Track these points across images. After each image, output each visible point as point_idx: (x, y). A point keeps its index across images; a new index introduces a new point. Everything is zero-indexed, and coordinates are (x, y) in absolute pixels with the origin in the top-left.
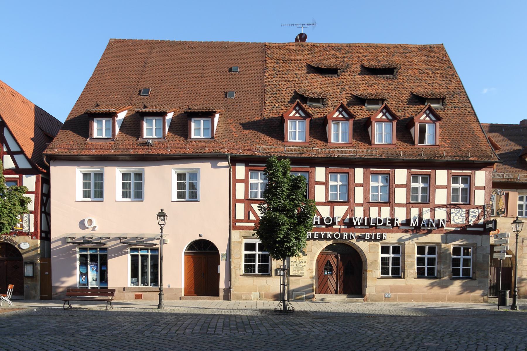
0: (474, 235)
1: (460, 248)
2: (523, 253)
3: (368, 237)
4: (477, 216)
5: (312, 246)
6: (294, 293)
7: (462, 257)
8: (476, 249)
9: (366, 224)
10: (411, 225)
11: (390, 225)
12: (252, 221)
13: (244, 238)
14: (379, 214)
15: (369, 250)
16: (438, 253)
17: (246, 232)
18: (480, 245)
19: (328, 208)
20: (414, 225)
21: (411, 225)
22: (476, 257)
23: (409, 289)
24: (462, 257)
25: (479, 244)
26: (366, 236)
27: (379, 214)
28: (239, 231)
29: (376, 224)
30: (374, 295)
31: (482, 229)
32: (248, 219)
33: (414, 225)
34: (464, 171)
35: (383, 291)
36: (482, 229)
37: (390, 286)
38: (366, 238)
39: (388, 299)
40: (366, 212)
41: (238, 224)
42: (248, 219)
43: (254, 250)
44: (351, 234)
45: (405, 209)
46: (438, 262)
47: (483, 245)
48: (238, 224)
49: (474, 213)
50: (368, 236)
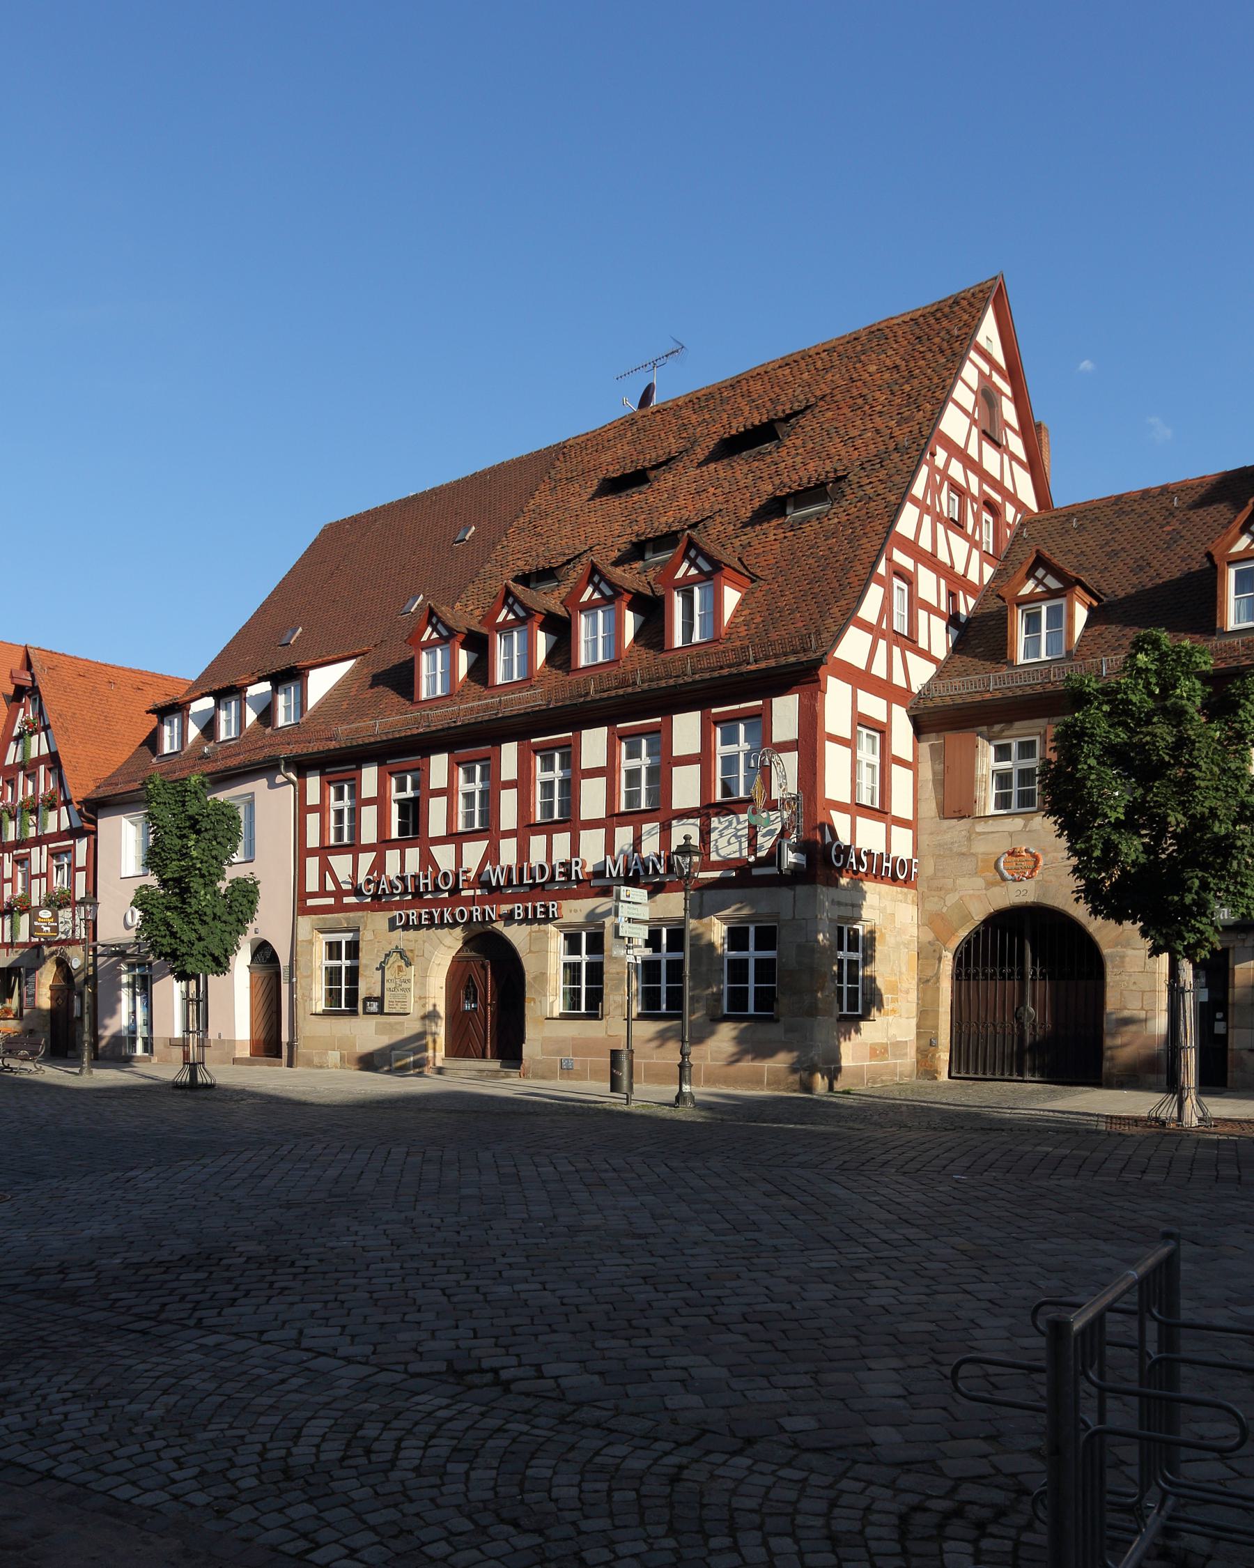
0: (774, 889)
1: (748, 928)
2: (1124, 930)
3: (519, 915)
4: (778, 832)
5: (424, 942)
6: (394, 1053)
7: (752, 954)
10: (608, 876)
11: (563, 879)
12: (329, 894)
13: (322, 932)
14: (575, 850)
18: (789, 917)
19: (451, 848)
21: (608, 876)
24: (752, 954)
25: (786, 915)
26: (516, 911)
27: (575, 850)
30: (540, 1062)
32: (323, 893)
33: (614, 874)
34: (742, 706)
35: (559, 1053)
37: (573, 1039)
38: (516, 918)
39: (568, 1074)
40: (523, 853)
41: (310, 902)
44: (487, 908)
48: (310, 902)
50: (520, 911)
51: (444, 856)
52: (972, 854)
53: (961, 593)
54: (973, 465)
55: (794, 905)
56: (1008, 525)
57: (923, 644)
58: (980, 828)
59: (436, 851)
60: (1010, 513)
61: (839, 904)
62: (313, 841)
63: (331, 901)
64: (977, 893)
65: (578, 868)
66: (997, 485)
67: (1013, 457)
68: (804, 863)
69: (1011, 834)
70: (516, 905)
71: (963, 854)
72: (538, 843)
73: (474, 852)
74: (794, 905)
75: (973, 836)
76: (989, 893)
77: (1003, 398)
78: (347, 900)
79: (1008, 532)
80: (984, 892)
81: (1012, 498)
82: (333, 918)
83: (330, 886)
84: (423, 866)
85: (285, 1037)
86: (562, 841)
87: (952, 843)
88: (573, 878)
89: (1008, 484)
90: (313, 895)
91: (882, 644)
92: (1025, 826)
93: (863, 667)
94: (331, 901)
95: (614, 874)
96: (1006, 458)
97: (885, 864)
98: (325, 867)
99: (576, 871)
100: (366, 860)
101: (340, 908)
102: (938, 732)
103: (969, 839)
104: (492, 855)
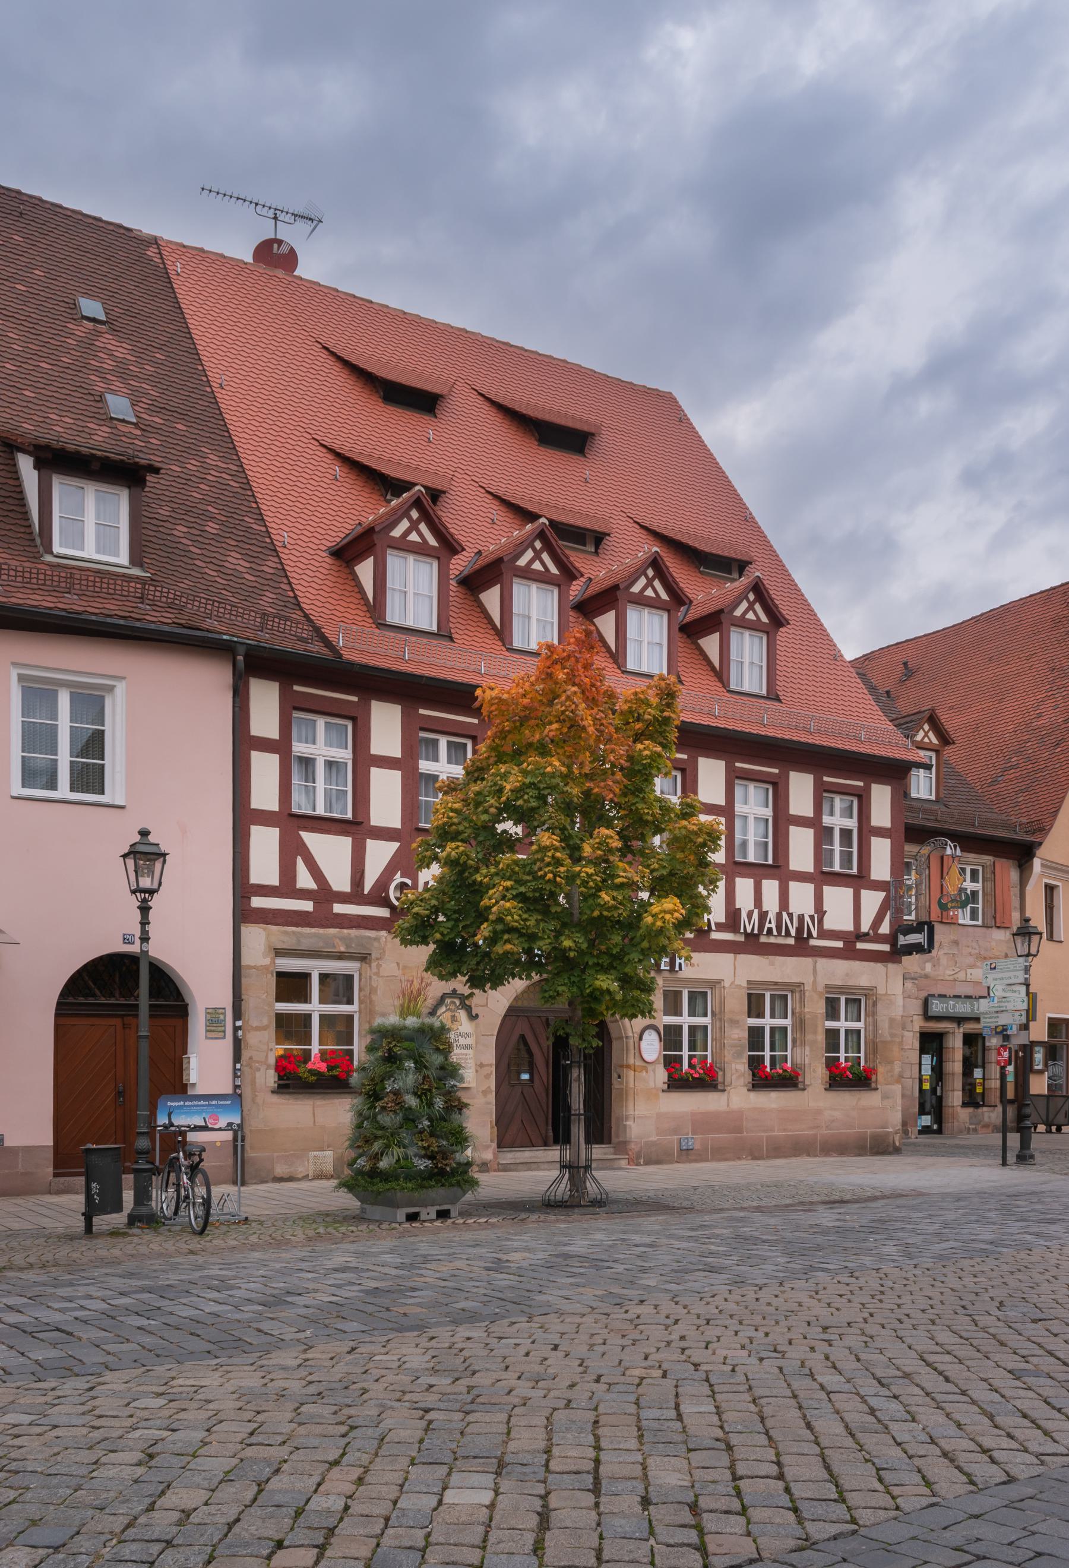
8: (875, 1004)
10: (742, 930)
12: (304, 894)
16: (793, 1013)
17: (286, 933)
20: (749, 930)
22: (875, 1024)
23: (733, 1123)
28: (264, 929)
30: (654, 1143)
31: (886, 948)
32: (287, 887)
33: (749, 930)
35: (675, 1131)
36: (886, 948)
37: (693, 1114)
39: (688, 1155)
41: (257, 902)
42: (287, 887)
43: (305, 998)
46: (794, 1041)
48: (257, 902)
63: (307, 906)
78: (339, 908)
82: (315, 935)
83: (305, 880)
88: (742, 930)
90: (343, 898)
94: (307, 906)
101: (322, 918)
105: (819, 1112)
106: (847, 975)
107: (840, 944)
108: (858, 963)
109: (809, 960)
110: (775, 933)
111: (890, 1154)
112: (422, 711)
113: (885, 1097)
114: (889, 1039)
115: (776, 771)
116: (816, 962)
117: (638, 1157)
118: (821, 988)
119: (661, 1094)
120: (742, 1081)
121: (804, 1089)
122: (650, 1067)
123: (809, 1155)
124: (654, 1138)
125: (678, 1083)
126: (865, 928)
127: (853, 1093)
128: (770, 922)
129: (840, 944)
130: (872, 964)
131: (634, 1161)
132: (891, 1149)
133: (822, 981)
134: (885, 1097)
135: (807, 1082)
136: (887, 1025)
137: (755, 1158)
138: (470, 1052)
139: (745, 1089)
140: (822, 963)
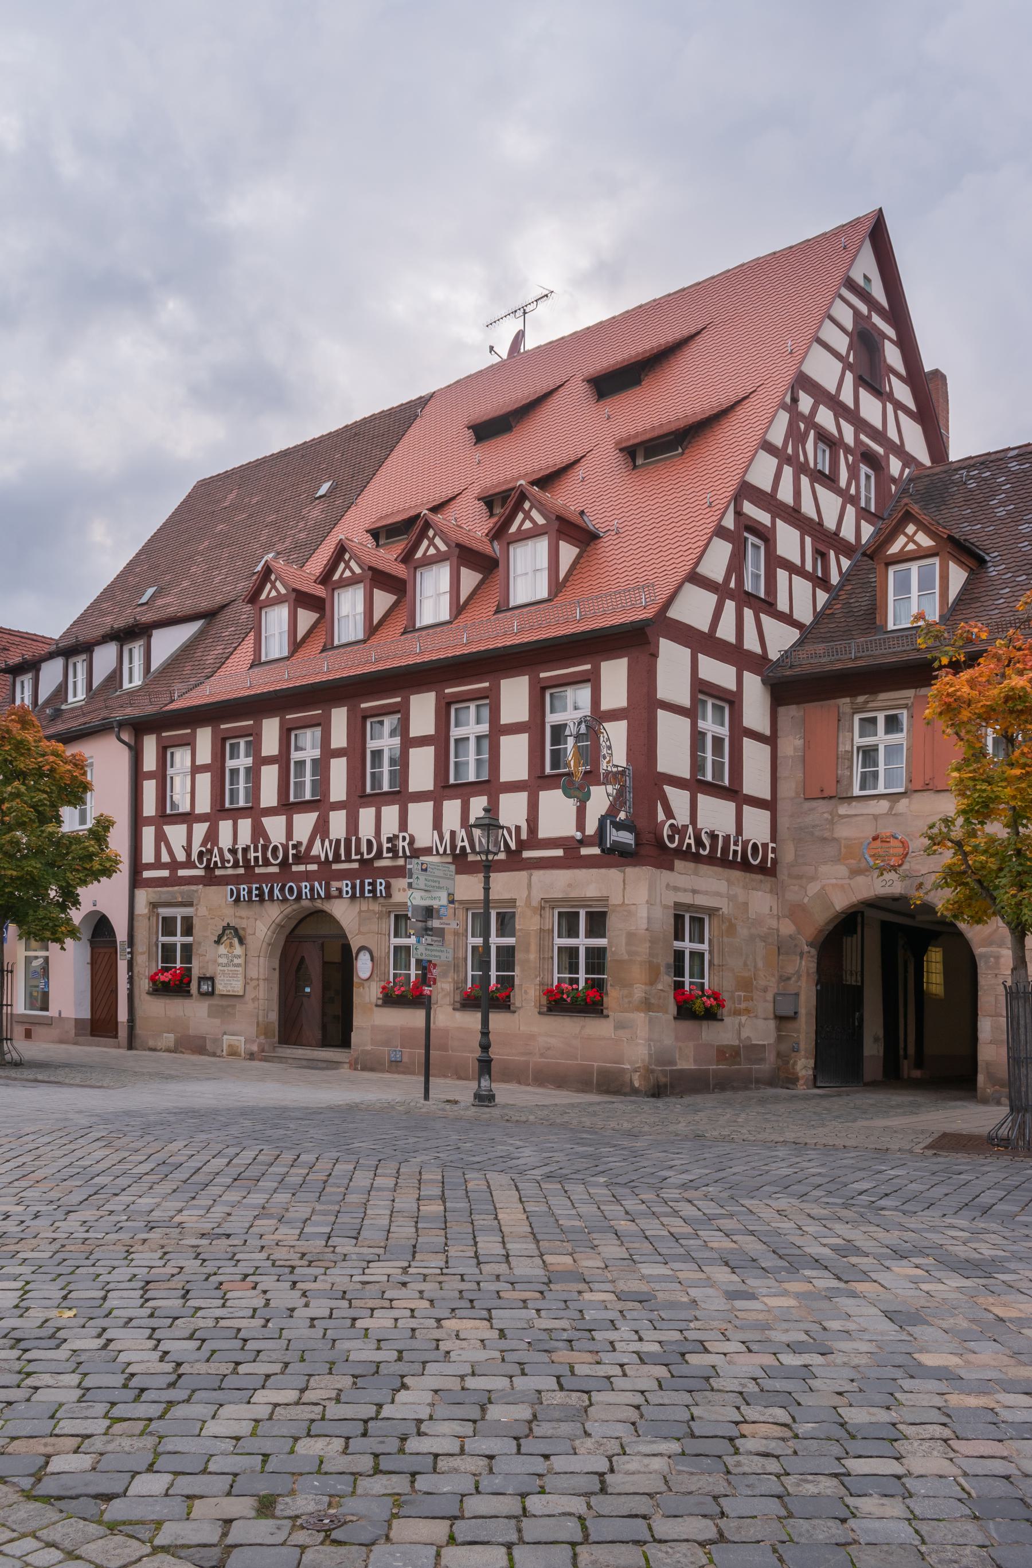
1: (578, 913)
3: (347, 892)
6: (225, 1037)
9: (343, 858)
14: (403, 825)
15: (357, 927)
19: (282, 819)
25: (615, 900)
26: (345, 889)
27: (403, 825)
29: (362, 854)
32: (158, 865)
33: (441, 851)
38: (345, 895)
41: (146, 874)
45: (430, 805)
47: (626, 902)
48: (146, 874)
49: (600, 798)
50: (349, 889)
51: (275, 827)
52: (835, 839)
53: (832, 553)
54: (852, 415)
55: (624, 888)
56: (894, 480)
57: (782, 605)
58: (843, 810)
59: (268, 822)
60: (895, 466)
61: (676, 889)
62: (149, 809)
63: (165, 873)
64: (840, 882)
65: (406, 844)
66: (879, 436)
67: (899, 406)
68: (632, 842)
69: (876, 817)
70: (345, 882)
71: (825, 839)
72: (366, 815)
73: (304, 823)
74: (624, 888)
75: (836, 819)
76: (852, 882)
77: (886, 341)
78: (182, 873)
79: (893, 487)
80: (847, 881)
81: (899, 451)
82: (168, 892)
83: (165, 858)
84: (255, 840)
85: (123, 1016)
86: (391, 813)
87: (814, 827)
88: (401, 854)
89: (892, 434)
91: (730, 606)
92: (891, 808)
93: (706, 629)
94: (165, 873)
95: (441, 851)
96: (890, 407)
97: (732, 847)
98: (161, 838)
99: (403, 847)
100: (200, 830)
101: (174, 881)
102: (798, 703)
103: (832, 822)
104: (321, 829)
105: (532, 1037)
106: (570, 885)
107: (559, 853)
108: (584, 871)
109: (523, 874)
110: (219, 865)
111: (625, 1094)
112: (222, 727)
113: (619, 1026)
114: (626, 957)
115: (487, 684)
116: (531, 875)
117: (356, 1063)
118: (535, 903)
119: (375, 1009)
120: (447, 1000)
121: (514, 1012)
122: (366, 984)
123: (519, 1083)
124: (369, 1048)
125: (391, 999)
126: (591, 827)
127: (575, 1019)
128: (463, 841)
129: (559, 853)
130: (603, 871)
131: (354, 1066)
132: (627, 1090)
133: (537, 896)
134: (619, 1026)
135: (518, 1004)
136: (623, 940)
137: (460, 1078)
138: (240, 969)
139: (450, 1009)
140: (538, 875)
